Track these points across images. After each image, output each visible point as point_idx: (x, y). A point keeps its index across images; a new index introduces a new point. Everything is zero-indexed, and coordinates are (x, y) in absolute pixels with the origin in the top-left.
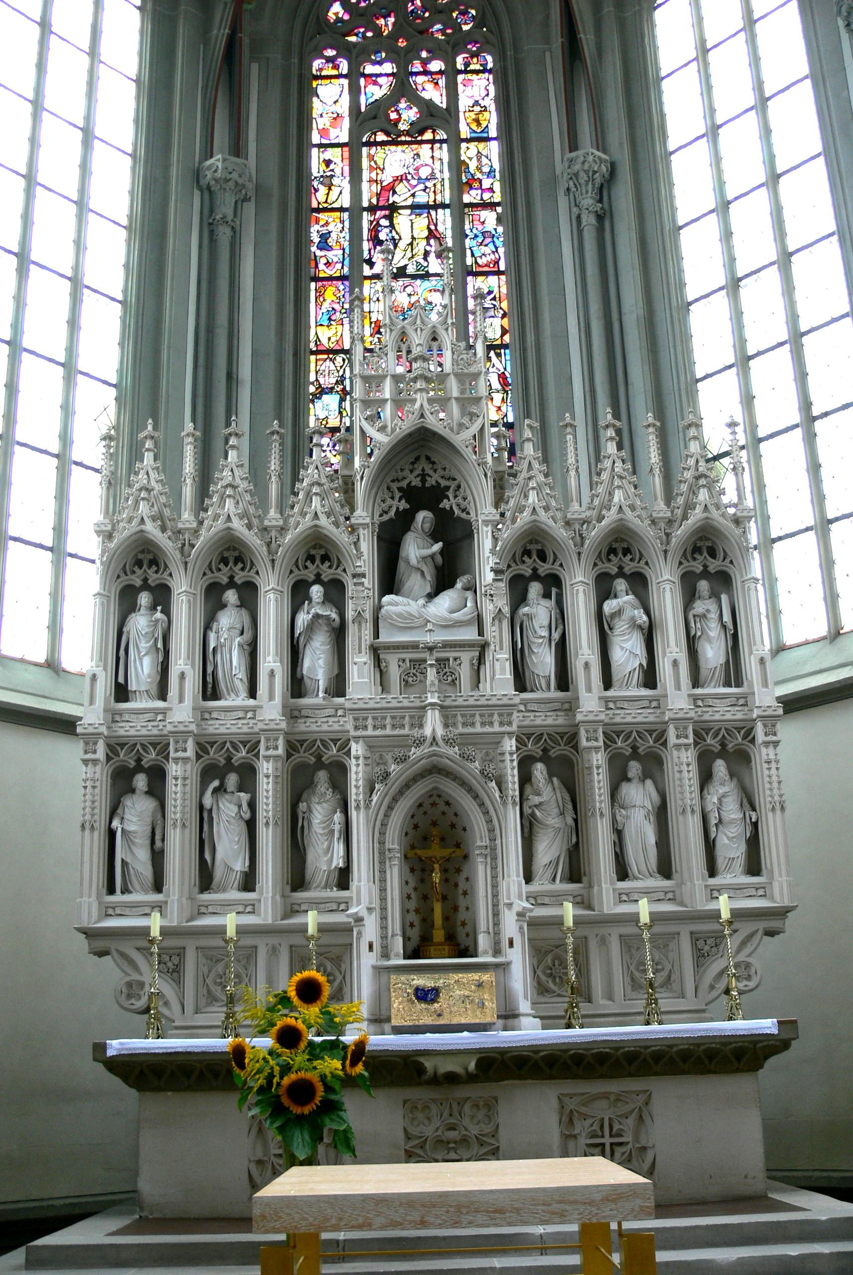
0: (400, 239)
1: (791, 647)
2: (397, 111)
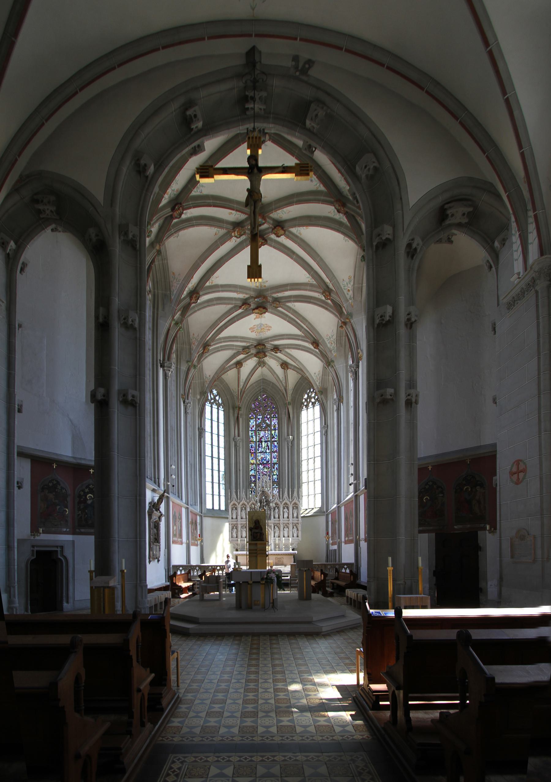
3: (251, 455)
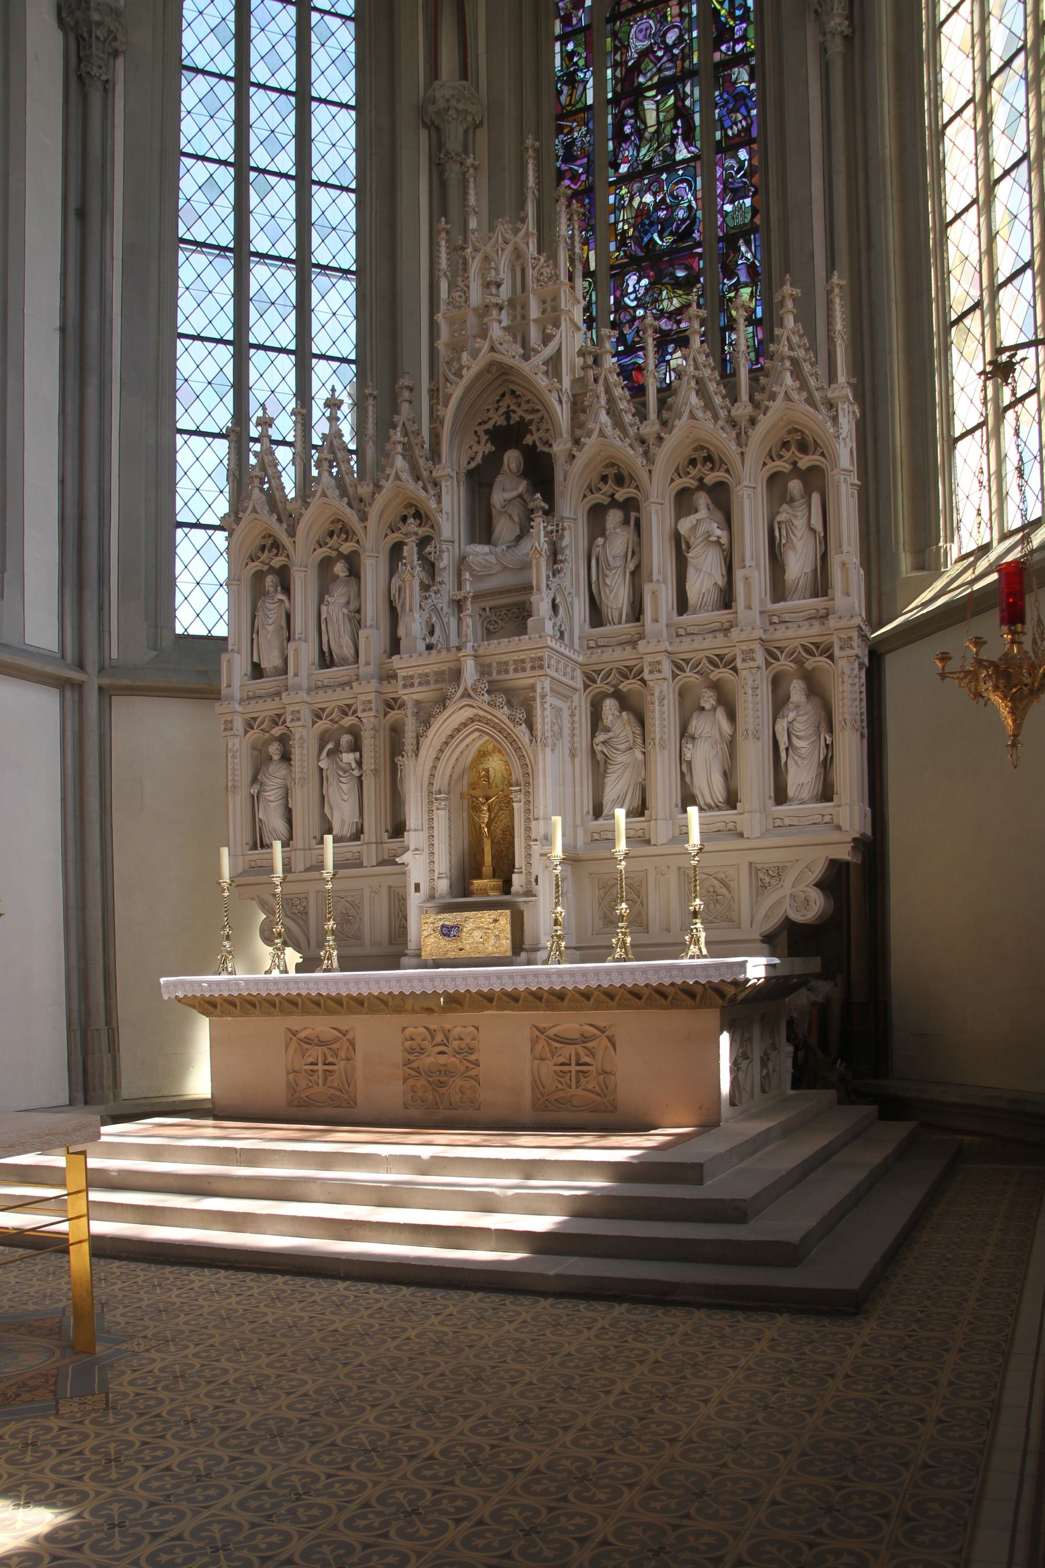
0: (646, 128)
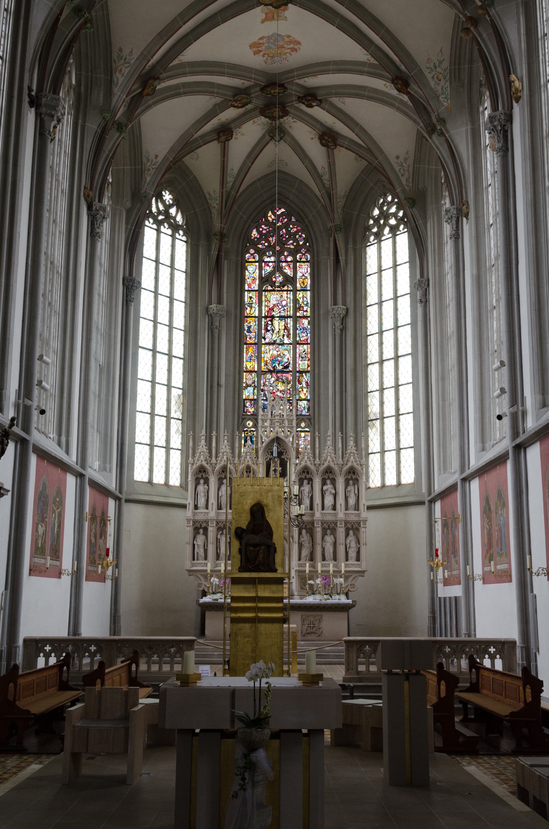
1: (387, 486)
2: (275, 277)
3: (247, 350)
